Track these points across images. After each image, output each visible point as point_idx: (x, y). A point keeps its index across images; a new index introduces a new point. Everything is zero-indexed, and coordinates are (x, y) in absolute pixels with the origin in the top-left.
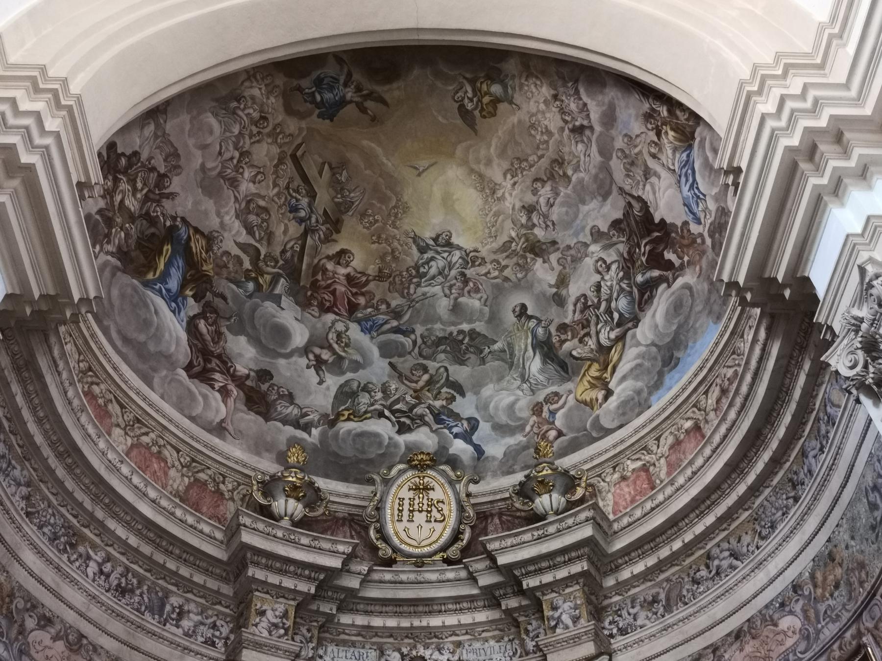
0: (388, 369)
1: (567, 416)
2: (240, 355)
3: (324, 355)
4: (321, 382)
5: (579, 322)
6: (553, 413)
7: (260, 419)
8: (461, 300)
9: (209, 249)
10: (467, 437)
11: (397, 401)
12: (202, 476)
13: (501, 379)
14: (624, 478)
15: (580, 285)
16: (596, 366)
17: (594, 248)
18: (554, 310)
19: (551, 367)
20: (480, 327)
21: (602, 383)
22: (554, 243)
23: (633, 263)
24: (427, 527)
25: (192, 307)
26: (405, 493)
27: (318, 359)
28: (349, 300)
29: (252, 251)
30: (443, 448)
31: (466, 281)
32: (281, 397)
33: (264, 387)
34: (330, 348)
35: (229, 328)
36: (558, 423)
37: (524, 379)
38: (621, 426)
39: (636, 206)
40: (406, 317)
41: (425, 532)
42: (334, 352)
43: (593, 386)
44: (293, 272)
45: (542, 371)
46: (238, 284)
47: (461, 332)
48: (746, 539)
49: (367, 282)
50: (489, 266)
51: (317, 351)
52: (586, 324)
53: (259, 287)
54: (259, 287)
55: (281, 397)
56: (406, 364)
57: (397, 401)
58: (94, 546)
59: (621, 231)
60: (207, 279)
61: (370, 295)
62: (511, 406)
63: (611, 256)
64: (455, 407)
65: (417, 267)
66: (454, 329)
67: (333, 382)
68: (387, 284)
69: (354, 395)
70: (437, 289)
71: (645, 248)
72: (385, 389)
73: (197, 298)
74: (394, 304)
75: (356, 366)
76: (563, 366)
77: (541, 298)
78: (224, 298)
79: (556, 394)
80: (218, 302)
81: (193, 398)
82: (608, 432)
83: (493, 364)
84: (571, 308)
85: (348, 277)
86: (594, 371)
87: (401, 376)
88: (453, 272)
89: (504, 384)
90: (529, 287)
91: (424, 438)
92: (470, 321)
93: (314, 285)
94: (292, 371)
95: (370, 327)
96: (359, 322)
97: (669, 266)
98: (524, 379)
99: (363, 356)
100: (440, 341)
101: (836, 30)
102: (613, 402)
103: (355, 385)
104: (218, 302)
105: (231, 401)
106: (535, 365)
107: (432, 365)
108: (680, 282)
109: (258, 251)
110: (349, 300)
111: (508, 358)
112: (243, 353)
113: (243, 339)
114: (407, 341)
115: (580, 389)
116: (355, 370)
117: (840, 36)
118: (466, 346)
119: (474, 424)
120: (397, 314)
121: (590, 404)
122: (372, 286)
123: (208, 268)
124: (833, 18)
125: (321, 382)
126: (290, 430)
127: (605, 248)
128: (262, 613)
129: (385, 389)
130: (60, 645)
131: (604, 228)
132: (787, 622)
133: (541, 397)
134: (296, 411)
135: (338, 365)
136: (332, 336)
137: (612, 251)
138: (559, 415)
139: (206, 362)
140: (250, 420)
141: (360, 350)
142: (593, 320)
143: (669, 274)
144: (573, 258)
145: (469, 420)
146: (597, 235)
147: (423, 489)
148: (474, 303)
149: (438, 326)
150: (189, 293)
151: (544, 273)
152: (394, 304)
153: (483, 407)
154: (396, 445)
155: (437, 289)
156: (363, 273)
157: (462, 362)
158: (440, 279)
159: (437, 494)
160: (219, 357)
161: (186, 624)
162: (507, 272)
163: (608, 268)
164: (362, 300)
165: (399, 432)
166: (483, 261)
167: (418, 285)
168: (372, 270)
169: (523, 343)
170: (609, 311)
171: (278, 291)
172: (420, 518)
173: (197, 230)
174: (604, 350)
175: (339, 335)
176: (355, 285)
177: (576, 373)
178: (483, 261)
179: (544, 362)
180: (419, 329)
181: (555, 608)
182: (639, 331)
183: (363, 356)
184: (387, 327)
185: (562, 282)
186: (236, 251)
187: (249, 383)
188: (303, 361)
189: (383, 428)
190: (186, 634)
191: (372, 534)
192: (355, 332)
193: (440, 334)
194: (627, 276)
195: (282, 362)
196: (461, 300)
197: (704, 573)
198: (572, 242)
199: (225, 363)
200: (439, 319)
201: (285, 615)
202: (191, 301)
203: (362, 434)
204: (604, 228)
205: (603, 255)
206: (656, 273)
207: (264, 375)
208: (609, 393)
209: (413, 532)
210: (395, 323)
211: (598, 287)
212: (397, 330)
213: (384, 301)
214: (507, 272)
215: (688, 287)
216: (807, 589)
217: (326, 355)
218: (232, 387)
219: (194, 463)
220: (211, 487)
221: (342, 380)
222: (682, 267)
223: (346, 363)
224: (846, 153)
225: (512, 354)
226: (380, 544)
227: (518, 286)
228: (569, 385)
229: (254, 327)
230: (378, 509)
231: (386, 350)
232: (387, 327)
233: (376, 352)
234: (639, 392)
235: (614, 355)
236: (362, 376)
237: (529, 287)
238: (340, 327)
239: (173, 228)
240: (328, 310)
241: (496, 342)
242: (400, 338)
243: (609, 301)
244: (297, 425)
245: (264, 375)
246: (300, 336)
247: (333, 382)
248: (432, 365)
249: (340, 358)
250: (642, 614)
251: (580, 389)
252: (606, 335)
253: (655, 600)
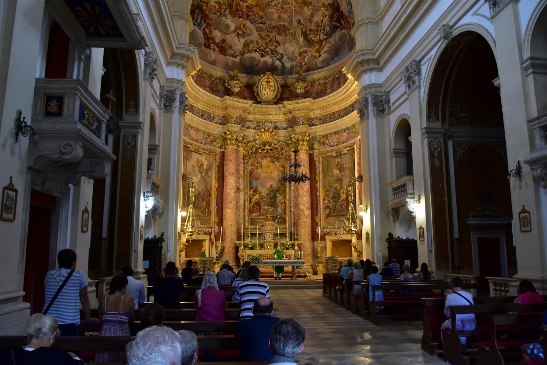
0: (258, 35)
1: (308, 59)
2: (217, 36)
3: (240, 32)
4: (239, 41)
5: (315, 30)
6: (304, 57)
7: (224, 56)
8: (281, 14)
9: (207, 6)
10: (280, 60)
11: (260, 46)
12: (213, 79)
13: (291, 42)
14: (320, 84)
15: (316, 19)
16: (318, 45)
17: (322, 9)
18: (309, 23)
19: (306, 41)
20: (286, 24)
21: (318, 51)
22: (311, 3)
23: (333, 18)
24: (269, 93)
25: (204, 25)
26: (264, 83)
27: (239, 34)
28: (247, 14)
29: (219, 3)
30: (273, 63)
31: (283, 9)
32: (228, 47)
33: (224, 45)
34: (241, 30)
35: (213, 29)
36: (306, 60)
37: (298, 44)
38: (322, 68)
39: (336, 3)
40: (264, 19)
41: (269, 94)
42: (243, 31)
43: (316, 52)
44: (230, 6)
45: (303, 42)
46: (215, 14)
47: (280, 25)
48: (342, 113)
49: (252, 8)
50: (291, 5)
51: (238, 31)
52: (317, 31)
53: (221, 13)
54: (221, 13)
55: (228, 47)
56: (263, 34)
57: (260, 46)
58: (196, 107)
59: (331, 7)
60: (207, 15)
61: (253, 12)
62: (293, 52)
63: (327, 13)
64: (277, 49)
65: (268, 3)
66: (278, 24)
67: (242, 41)
68: (258, 8)
69: (248, 44)
70: (274, 10)
71: (336, 16)
72: (257, 43)
73: (204, 22)
74: (260, 14)
75: (249, 35)
76: (309, 42)
77: (305, 18)
78: (211, 19)
79: (306, 51)
80: (210, 21)
81: (207, 55)
82: (318, 68)
83: (289, 37)
84: (313, 24)
85: (247, 6)
86: (317, 47)
87: (262, 38)
88: (279, 5)
89: (292, 44)
90: (302, 14)
91: (268, 59)
92: (283, 22)
93: (237, 10)
94: (231, 39)
95: (253, 22)
96: (250, 20)
97: (341, 24)
98: (298, 44)
99: (251, 31)
100: (274, 27)
101: (381, 17)
102: (321, 59)
103: (249, 41)
104: (210, 21)
105: (216, 52)
106: (301, 40)
107: (271, 35)
108: (343, 31)
109: (220, 2)
110: (247, 14)
111: (293, 35)
112: (217, 35)
113: (217, 31)
114: (264, 27)
115: (312, 52)
116: (249, 36)
117: (382, 18)
118: (281, 30)
119: (282, 56)
120: (261, 18)
121: (315, 57)
122: (254, 9)
123: (207, 12)
124: (381, 14)
125: (239, 41)
126: (232, 59)
127: (326, 10)
128: (232, 118)
129: (257, 43)
130: (195, 132)
131: (326, 4)
132: (344, 134)
133: (302, 51)
134: (233, 52)
135: (244, 35)
136: (242, 26)
137: (327, 12)
138: (306, 58)
139: (209, 41)
140: (221, 57)
141: (250, 29)
142: (319, 31)
143: (341, 27)
144: (316, 10)
145: (281, 54)
146: (324, 5)
147: (268, 82)
148: (285, 16)
149: (274, 22)
150: (203, 21)
151: (307, 11)
152: (260, 14)
153: (285, 50)
154: (259, 61)
155: (274, 10)
156: (251, 5)
157: (280, 35)
158: (275, 7)
159: (272, 84)
160: (212, 39)
161: (215, 120)
162: (296, 8)
163: (326, 16)
164: (251, 13)
165: (261, 57)
166: (289, 4)
167: (268, 9)
168: (254, 4)
169: (299, 32)
170: (324, 29)
171: (226, 13)
172: (267, 90)
173: (204, 2)
174: (321, 41)
175: (244, 25)
176: (249, 9)
177: (312, 45)
178: (289, 4)
179: (304, 39)
180: (268, 23)
181: (298, 119)
182: (331, 39)
183: (251, 31)
184: (258, 22)
185: (312, 15)
186: (214, 4)
187: (220, 45)
188: (234, 35)
189: (256, 55)
190: (216, 123)
191: (256, 94)
192: (249, 24)
193: (274, 25)
194: (330, 21)
195: (228, 36)
196: (281, 14)
197: (332, 116)
198: (317, 5)
199: (213, 39)
200: (274, 20)
201: (237, 118)
202: (203, 24)
203: (252, 58)
204: (326, 4)
205: (325, 12)
206: (338, 24)
207: (224, 41)
208: (320, 56)
209: (266, 94)
210: (260, 21)
211: (322, 21)
212: (261, 23)
213: (257, 13)
214: (296, 8)
215: (344, 33)
216: (349, 130)
217: (240, 32)
218: (216, 48)
219: (210, 76)
220: (215, 82)
221: (245, 40)
222: (345, 27)
223: (246, 34)
224: (369, 65)
225: (295, 35)
226: (257, 97)
227: (299, 13)
228: (310, 49)
229: (220, 27)
230: (257, 87)
231: (258, 30)
232: (258, 22)
233: (255, 30)
234: (328, 58)
235: (323, 44)
236: (251, 38)
237: (302, 14)
238: (244, 22)
239: (199, 4)
240: (241, 17)
241: (290, 30)
242: (262, 25)
243: (324, 26)
244: (233, 57)
245: (224, 41)
246: (232, 28)
247: (242, 41)
248: (271, 35)
249: (244, 33)
250: (318, 122)
251: (313, 51)
252: (322, 37)
253: (321, 119)
